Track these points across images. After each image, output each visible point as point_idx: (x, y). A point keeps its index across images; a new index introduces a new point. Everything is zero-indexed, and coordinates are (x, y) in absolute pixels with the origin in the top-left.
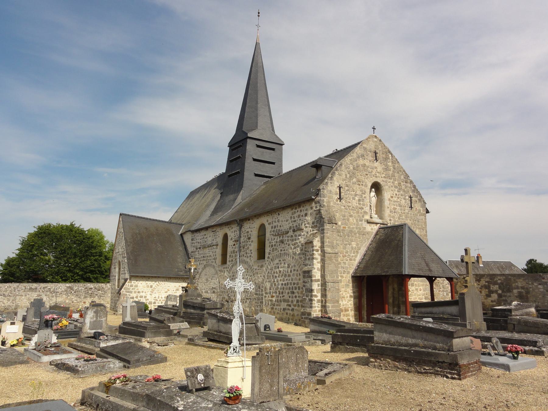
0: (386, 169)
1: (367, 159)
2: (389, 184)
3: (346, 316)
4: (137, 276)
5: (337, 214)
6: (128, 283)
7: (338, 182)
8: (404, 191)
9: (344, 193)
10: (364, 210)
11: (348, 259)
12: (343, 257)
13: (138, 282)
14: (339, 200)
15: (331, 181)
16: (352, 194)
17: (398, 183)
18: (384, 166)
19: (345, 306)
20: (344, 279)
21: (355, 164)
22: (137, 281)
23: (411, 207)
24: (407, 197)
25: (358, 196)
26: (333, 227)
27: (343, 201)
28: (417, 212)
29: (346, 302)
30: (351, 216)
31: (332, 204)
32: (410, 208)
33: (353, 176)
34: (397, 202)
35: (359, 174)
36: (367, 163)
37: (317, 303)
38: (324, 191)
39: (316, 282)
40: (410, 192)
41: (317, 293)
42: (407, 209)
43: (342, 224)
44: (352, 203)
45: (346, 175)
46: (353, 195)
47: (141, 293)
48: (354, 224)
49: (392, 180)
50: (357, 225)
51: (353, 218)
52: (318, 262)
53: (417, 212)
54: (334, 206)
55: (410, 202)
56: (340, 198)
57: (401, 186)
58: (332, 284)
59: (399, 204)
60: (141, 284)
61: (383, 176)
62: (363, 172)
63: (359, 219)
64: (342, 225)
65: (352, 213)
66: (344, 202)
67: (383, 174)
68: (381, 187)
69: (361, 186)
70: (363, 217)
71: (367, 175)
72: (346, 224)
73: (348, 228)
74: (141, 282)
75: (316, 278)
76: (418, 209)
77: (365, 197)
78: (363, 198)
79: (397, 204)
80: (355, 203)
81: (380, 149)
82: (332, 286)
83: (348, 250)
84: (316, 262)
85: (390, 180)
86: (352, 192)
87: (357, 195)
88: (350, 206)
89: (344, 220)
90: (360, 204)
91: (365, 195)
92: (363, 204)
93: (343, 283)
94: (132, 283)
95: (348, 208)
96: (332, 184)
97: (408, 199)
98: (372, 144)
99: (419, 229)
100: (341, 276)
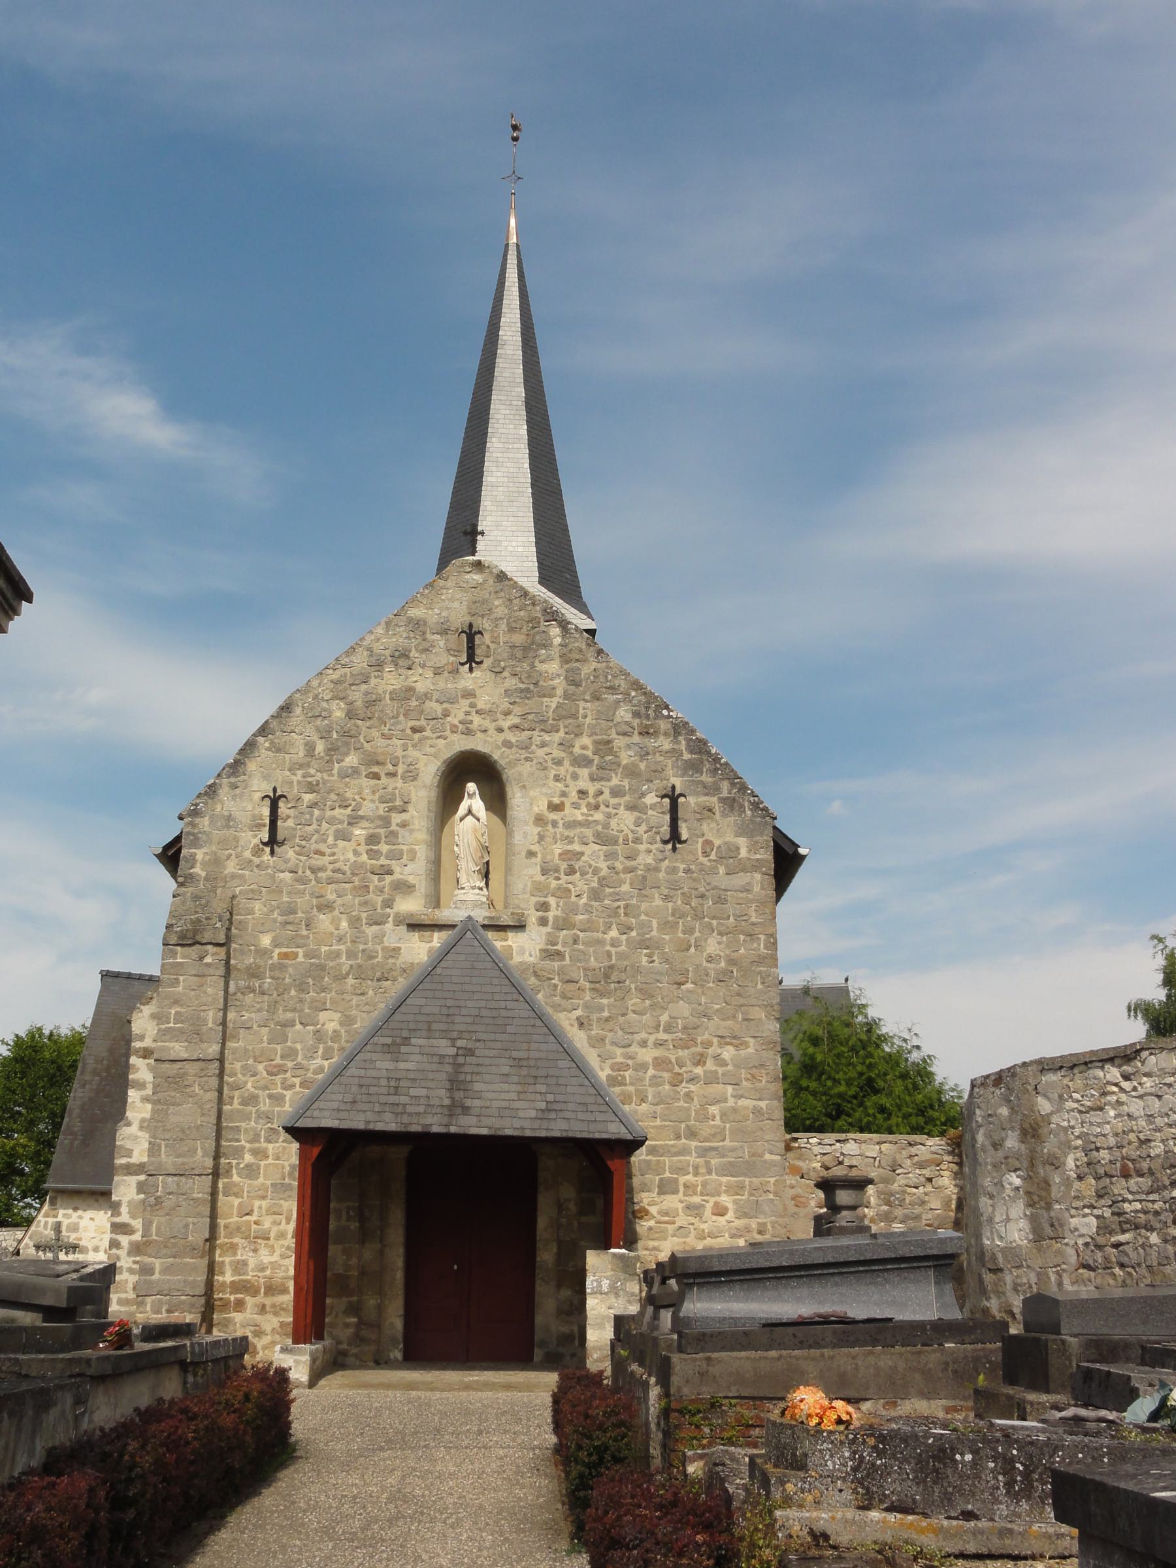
0: (527, 690)
1: (423, 666)
2: (541, 752)
3: (276, 1314)
4: (78, 1193)
5: (257, 906)
6: (47, 1215)
7: (266, 777)
8: (631, 772)
9: (296, 817)
10: (396, 876)
11: (297, 1081)
12: (270, 1074)
13: (80, 1212)
14: (268, 849)
15: (233, 780)
16: (334, 817)
17: (595, 742)
18: (511, 683)
19: (268, 1272)
20: (270, 1161)
21: (357, 695)
22: (76, 1209)
23: (675, 837)
24: (651, 799)
25: (365, 824)
26: (201, 959)
27: (288, 852)
28: (713, 857)
29: (278, 1253)
30: (326, 907)
31: (231, 867)
32: (665, 842)
33: (347, 744)
34: (586, 824)
35: (375, 733)
36: (422, 681)
37: (129, 1254)
38: (197, 820)
39: (130, 1174)
40: (669, 772)
41: (134, 1217)
42: (648, 853)
43: (276, 944)
44: (333, 854)
45: (310, 748)
46: (341, 822)
47: (91, 1253)
48: (340, 939)
49: (561, 734)
50: (353, 942)
51: (336, 912)
52: (145, 1099)
53: (713, 857)
54: (242, 877)
55: (667, 817)
56: (273, 842)
57: (611, 751)
58: (170, 1179)
59: (597, 835)
60: (92, 1219)
61: (506, 724)
62: (399, 723)
63: (364, 915)
64: (276, 946)
65: (331, 897)
66: (291, 854)
67: (507, 713)
68: (443, 773)
69: (384, 780)
70: (388, 904)
71: (415, 730)
72: (295, 940)
73: (306, 956)
74: (90, 1214)
75: (132, 1160)
76: (717, 842)
77: (404, 825)
78: (394, 827)
79: (588, 833)
80: (347, 854)
81: (500, 610)
82: (173, 1188)
83: (299, 1046)
84: (137, 1100)
85: (547, 737)
86: (337, 811)
87: (362, 817)
88: (322, 869)
89: (290, 927)
90: (372, 854)
91: (404, 816)
92: (390, 851)
93: (261, 1180)
94: (60, 1215)
95: (312, 877)
96: (238, 791)
97: (653, 807)
98: (452, 600)
99: (721, 934)
100: (255, 1152)
